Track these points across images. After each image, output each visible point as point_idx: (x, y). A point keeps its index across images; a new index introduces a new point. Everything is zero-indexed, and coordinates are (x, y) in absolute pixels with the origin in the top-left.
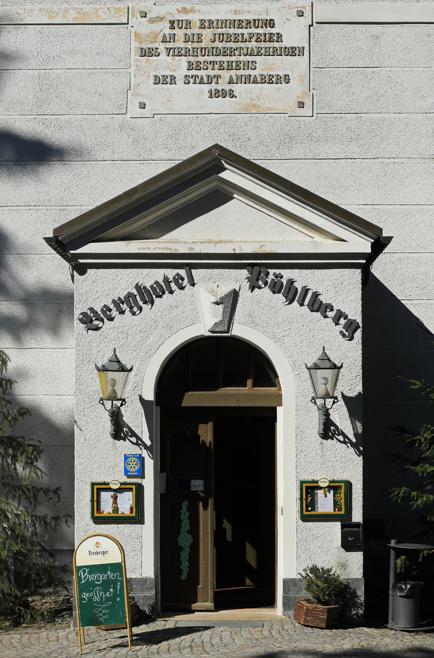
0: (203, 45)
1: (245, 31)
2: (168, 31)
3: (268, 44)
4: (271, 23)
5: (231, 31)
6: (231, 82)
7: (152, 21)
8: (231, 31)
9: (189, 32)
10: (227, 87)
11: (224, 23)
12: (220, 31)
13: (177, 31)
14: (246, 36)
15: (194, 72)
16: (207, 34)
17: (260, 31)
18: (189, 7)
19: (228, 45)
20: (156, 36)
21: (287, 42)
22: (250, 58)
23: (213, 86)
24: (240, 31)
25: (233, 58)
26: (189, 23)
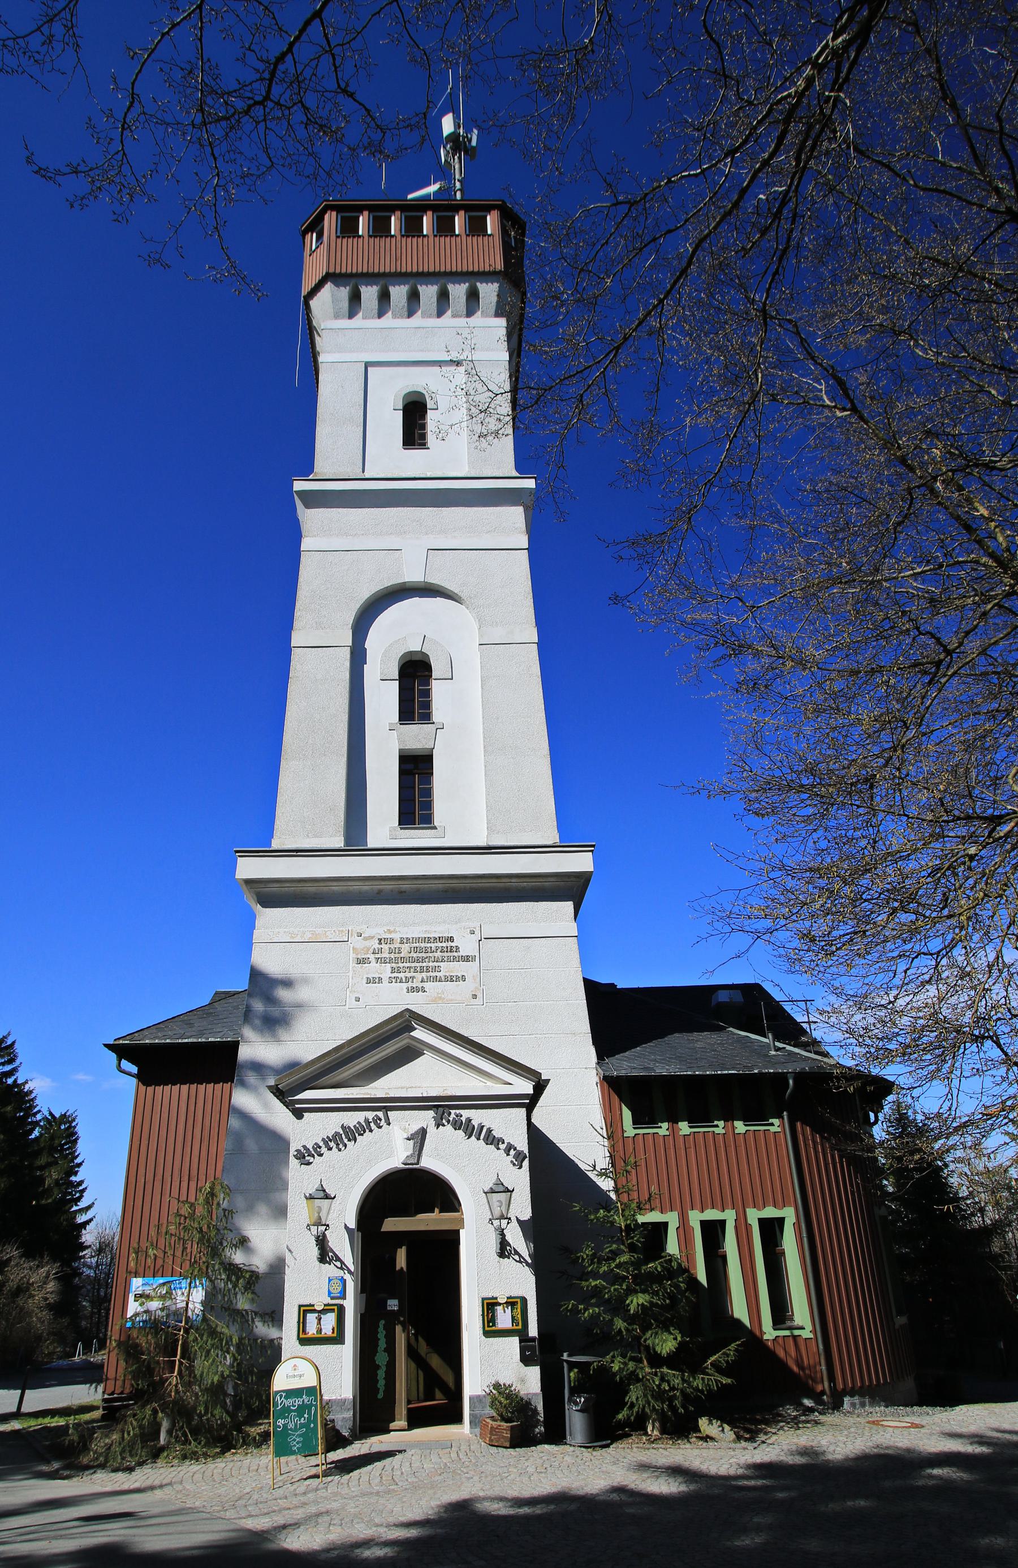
0: (402, 955)
1: (433, 945)
2: (377, 946)
3: (449, 954)
5: (423, 945)
7: (365, 939)
8: (423, 945)
9: (392, 946)
10: (420, 985)
11: (418, 940)
12: (415, 945)
15: (394, 975)
16: (405, 948)
19: (420, 955)
20: (368, 949)
23: (410, 984)
24: (429, 945)
25: (424, 964)
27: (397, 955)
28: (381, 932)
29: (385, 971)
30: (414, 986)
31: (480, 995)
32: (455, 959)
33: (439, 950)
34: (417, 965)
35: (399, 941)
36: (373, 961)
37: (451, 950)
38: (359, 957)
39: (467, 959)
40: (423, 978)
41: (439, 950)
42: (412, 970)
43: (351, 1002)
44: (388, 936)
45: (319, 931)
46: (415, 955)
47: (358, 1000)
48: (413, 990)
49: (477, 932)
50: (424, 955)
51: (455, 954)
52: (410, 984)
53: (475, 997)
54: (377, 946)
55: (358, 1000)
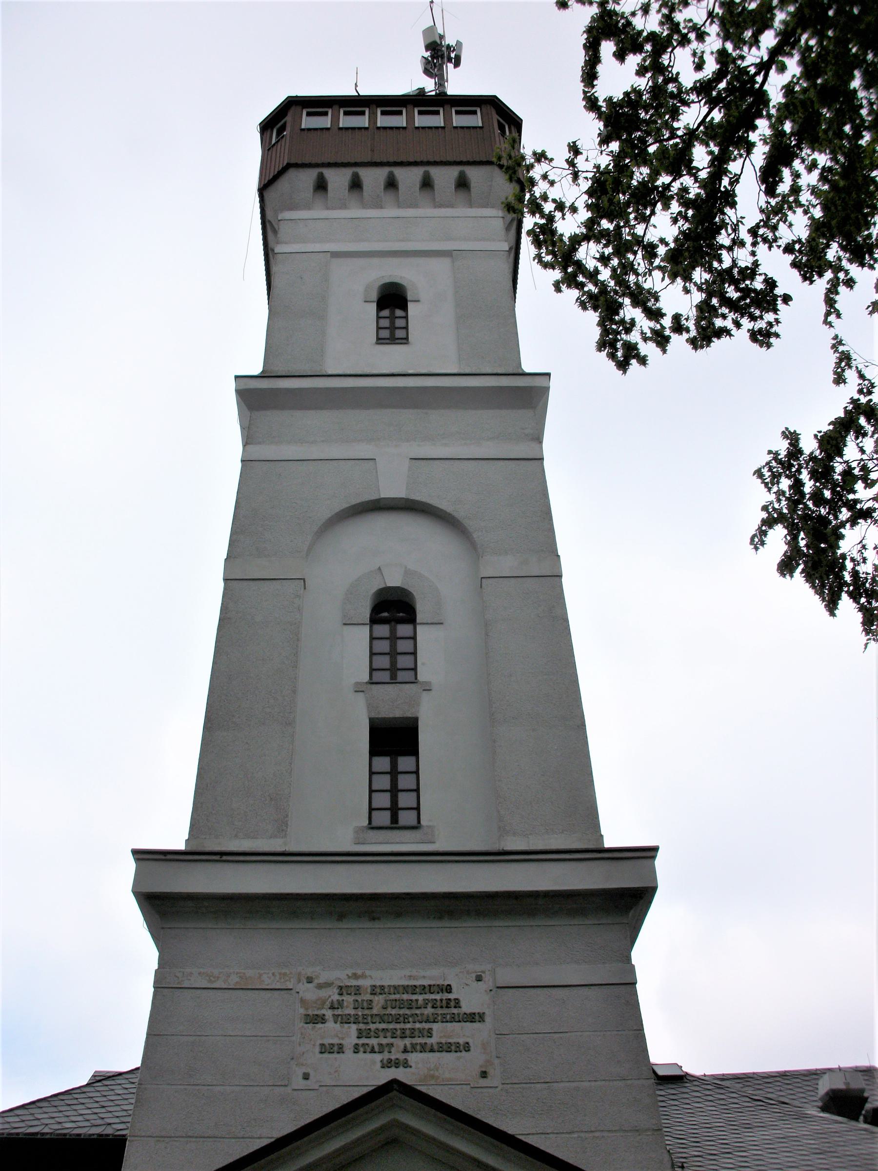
0: (375, 1011)
1: (420, 998)
2: (336, 997)
3: (445, 1011)
4: (449, 989)
5: (405, 997)
6: (405, 1051)
7: (320, 986)
8: (405, 997)
9: (359, 998)
10: (402, 1057)
11: (396, 989)
12: (393, 997)
13: (346, 998)
14: (420, 1002)
15: (364, 1041)
16: (379, 1000)
17: (438, 997)
18: (359, 972)
19: (402, 1012)
20: (324, 1002)
21: (467, 1007)
22: (427, 1026)
23: (386, 1056)
24: (414, 997)
25: (408, 1026)
26: (358, 988)
27: (366, 1012)
28: (341, 976)
29: (350, 1035)
30: (393, 1057)
31: (491, 1071)
32: (454, 1019)
33: (430, 1005)
34: (398, 1026)
35: (369, 990)
36: (331, 1019)
37: (448, 1003)
38: (310, 1012)
39: (473, 1018)
40: (405, 1047)
41: (430, 1005)
42: (389, 1034)
43: (298, 1082)
44: (354, 983)
45: (250, 973)
46: (393, 1012)
47: (306, 1077)
48: (388, 1064)
49: (487, 977)
50: (408, 1012)
51: (455, 1011)
52: (386, 1056)
53: (484, 1075)
54: (336, 997)
55: (306, 1077)
